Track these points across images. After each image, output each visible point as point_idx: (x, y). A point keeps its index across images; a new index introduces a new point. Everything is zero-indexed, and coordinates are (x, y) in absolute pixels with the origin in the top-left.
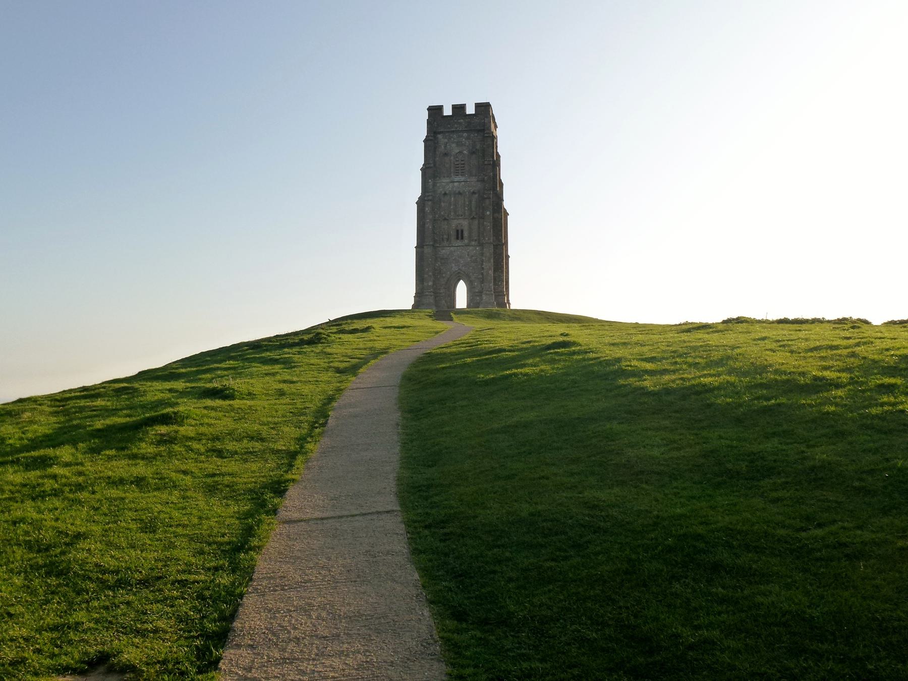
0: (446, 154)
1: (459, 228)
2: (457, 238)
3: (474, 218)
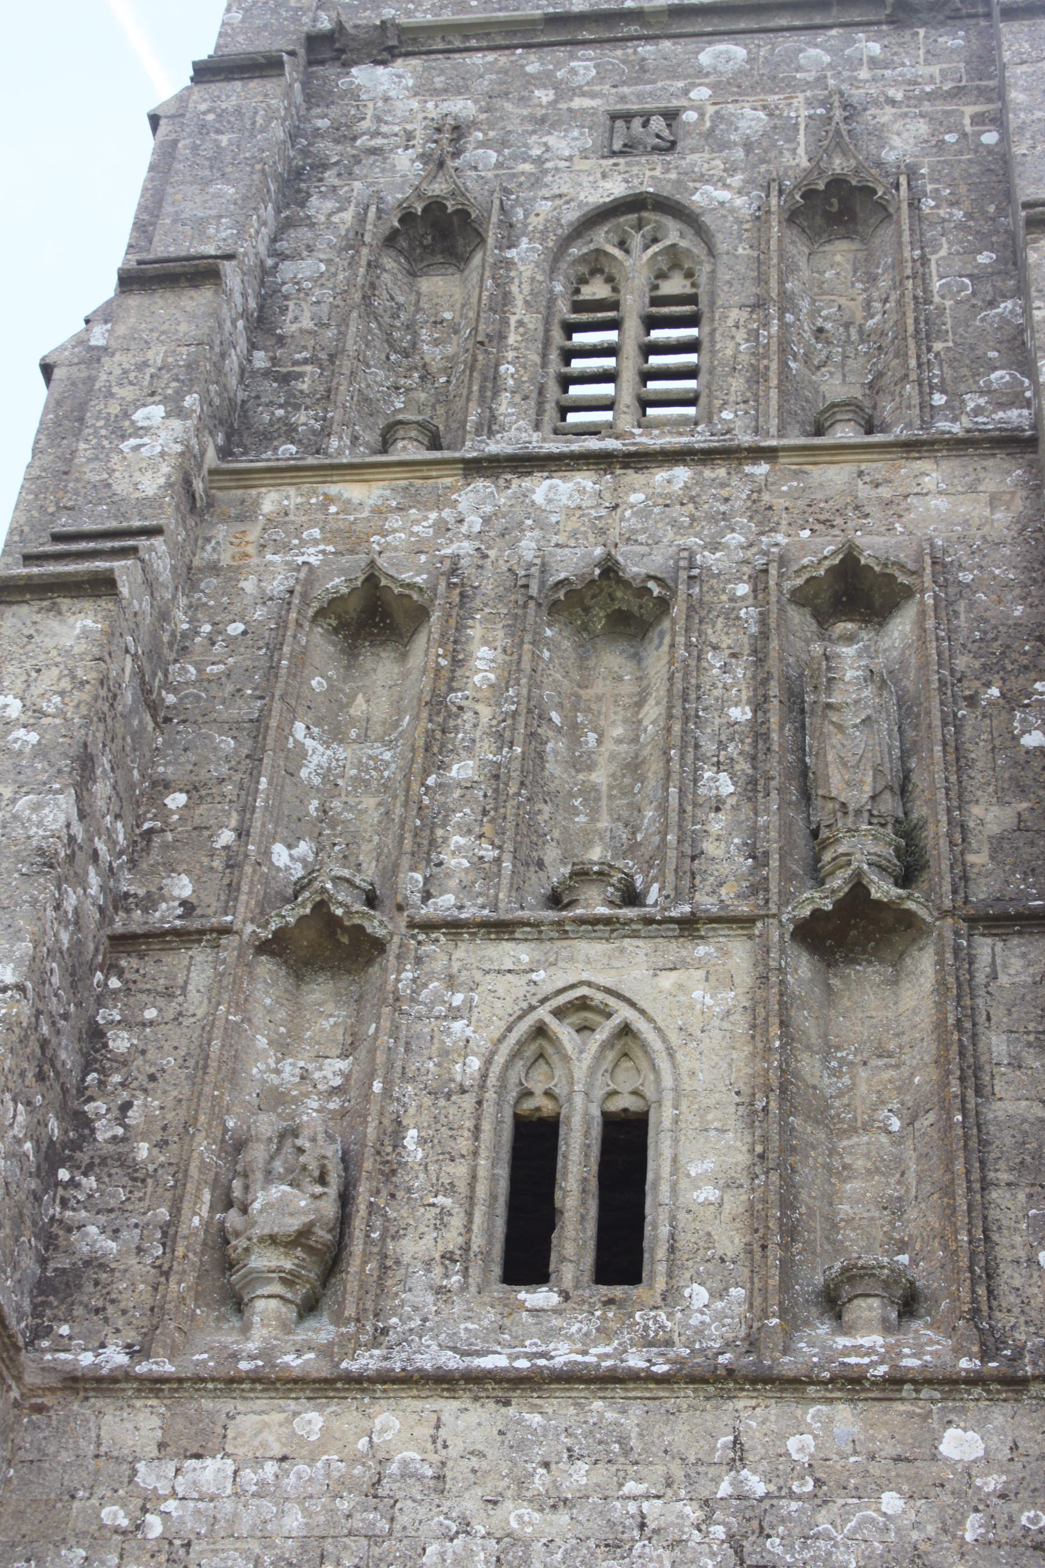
0: (439, 232)
1: (581, 1092)
2: (526, 1259)
3: (849, 932)
